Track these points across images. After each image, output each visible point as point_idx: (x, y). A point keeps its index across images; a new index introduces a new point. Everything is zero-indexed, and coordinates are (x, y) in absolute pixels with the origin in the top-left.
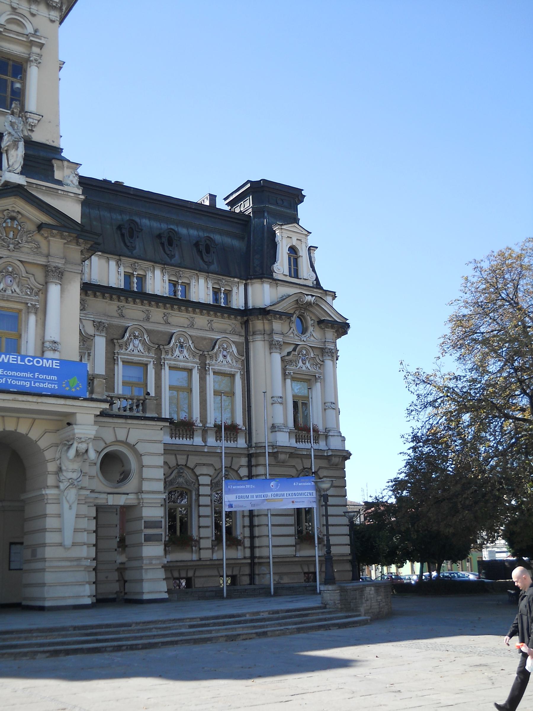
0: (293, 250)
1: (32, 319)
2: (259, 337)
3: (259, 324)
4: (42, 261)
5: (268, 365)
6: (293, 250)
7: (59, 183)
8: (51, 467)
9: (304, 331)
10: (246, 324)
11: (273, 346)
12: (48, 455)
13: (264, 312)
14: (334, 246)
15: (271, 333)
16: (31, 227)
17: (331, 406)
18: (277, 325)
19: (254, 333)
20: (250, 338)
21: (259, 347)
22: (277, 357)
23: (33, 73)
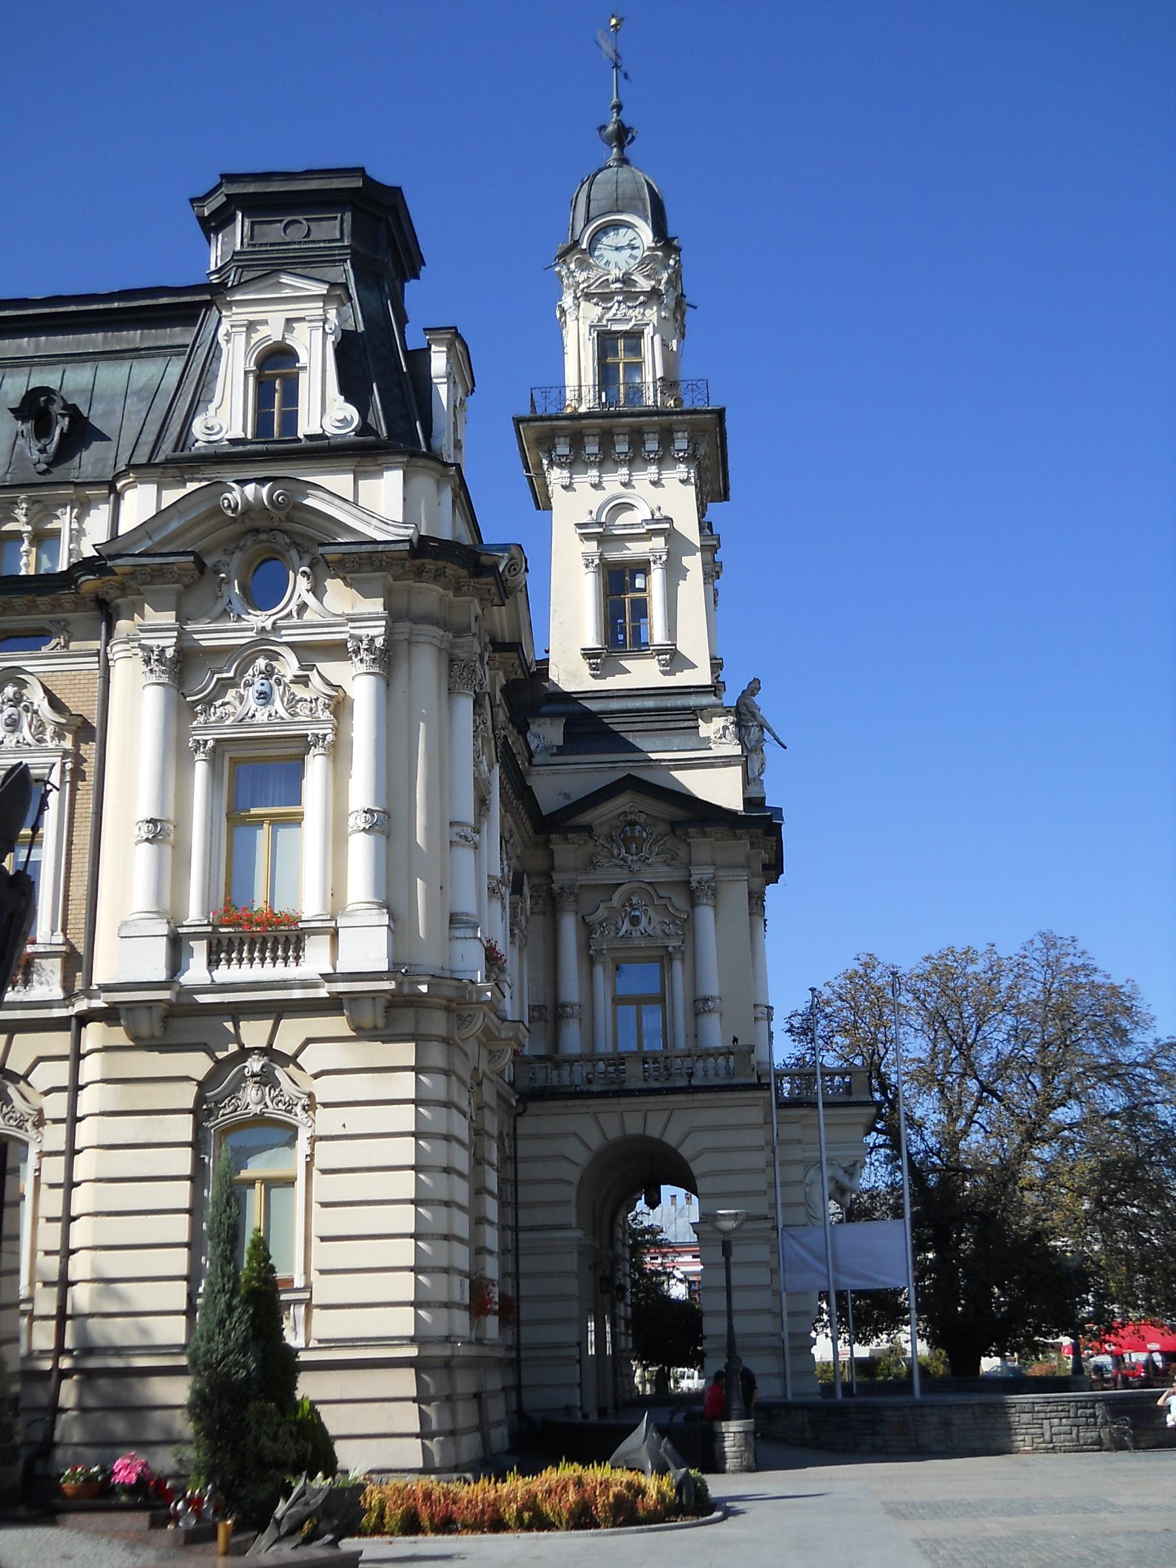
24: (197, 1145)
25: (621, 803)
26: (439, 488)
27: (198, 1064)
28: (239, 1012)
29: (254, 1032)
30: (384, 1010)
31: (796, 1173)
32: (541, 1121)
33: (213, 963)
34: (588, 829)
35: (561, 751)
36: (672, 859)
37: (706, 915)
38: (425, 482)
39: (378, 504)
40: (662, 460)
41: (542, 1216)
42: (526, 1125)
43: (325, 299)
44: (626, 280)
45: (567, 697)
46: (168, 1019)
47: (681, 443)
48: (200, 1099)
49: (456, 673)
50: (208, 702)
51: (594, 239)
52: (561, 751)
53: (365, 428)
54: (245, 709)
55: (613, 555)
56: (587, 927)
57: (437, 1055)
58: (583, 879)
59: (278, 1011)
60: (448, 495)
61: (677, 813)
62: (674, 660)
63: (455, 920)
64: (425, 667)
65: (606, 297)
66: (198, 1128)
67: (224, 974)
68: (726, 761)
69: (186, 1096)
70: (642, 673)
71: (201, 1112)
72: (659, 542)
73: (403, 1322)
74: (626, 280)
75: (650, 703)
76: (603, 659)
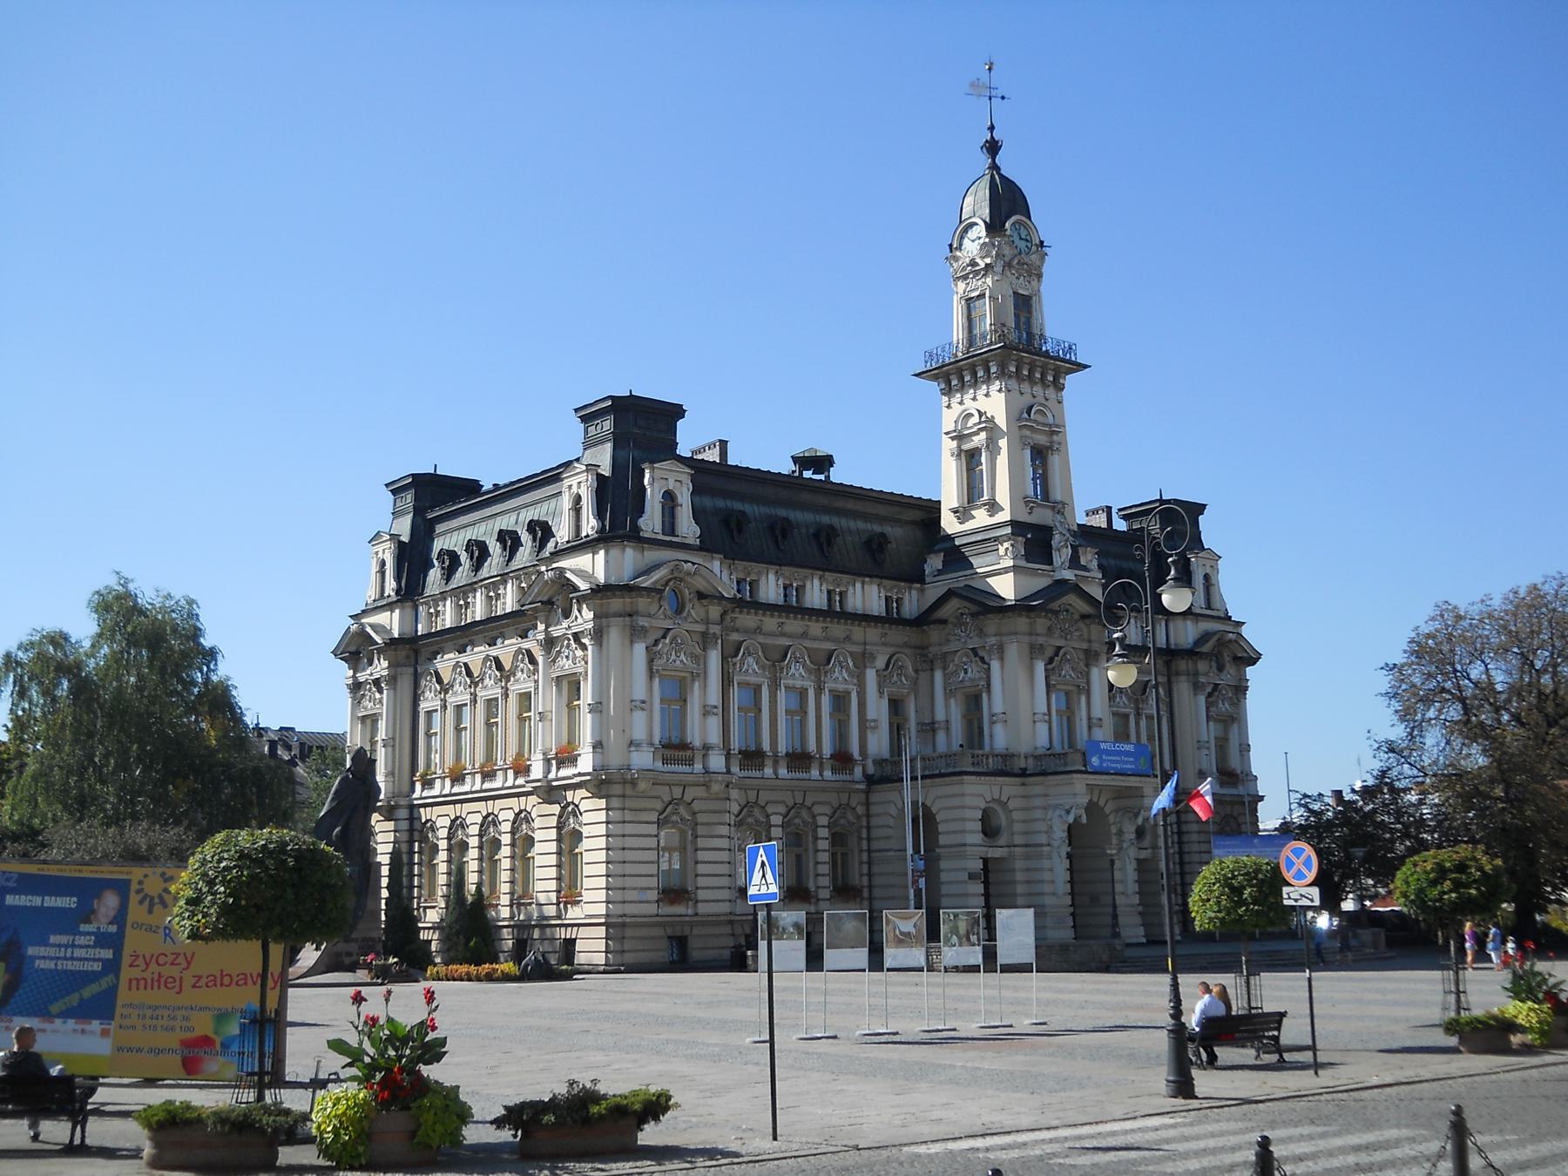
0: (1207, 577)
1: (1083, 699)
2: (1183, 678)
3: (1183, 665)
4: (1085, 646)
5: (1192, 706)
6: (1207, 577)
7: (1085, 569)
8: (1114, 830)
9: (1221, 669)
10: (1168, 664)
11: (1197, 687)
12: (1111, 818)
13: (1191, 653)
14: (1251, 576)
15: (1196, 674)
16: (1076, 616)
17: (1245, 748)
18: (1202, 666)
19: (1178, 674)
20: (1173, 679)
21: (1183, 688)
22: (1202, 699)
23: (1055, 461)
24: (559, 840)
25: (953, 605)
26: (623, 551)
27: (556, 809)
28: (566, 788)
29: (569, 794)
30: (600, 784)
31: (1038, 814)
32: (881, 795)
33: (558, 769)
34: (944, 622)
35: (940, 573)
36: (981, 633)
37: (995, 665)
38: (615, 552)
39: (592, 567)
40: (988, 380)
41: (882, 845)
42: (874, 798)
43: (587, 471)
44: (973, 263)
45: (950, 538)
46: (550, 793)
47: (993, 369)
48: (559, 822)
49: (635, 633)
50: (554, 661)
51: (962, 238)
52: (940, 573)
53: (601, 530)
54: (565, 665)
55: (966, 447)
56: (946, 677)
57: (615, 803)
58: (945, 649)
59: (575, 787)
60: (629, 552)
61: (974, 608)
62: (993, 507)
63: (631, 743)
64: (614, 636)
65: (965, 277)
66: (559, 834)
67: (564, 772)
68: (1006, 570)
69: (553, 821)
70: (981, 518)
71: (559, 828)
72: (983, 435)
73: (601, 909)
74: (973, 263)
75: (979, 537)
76: (962, 514)
